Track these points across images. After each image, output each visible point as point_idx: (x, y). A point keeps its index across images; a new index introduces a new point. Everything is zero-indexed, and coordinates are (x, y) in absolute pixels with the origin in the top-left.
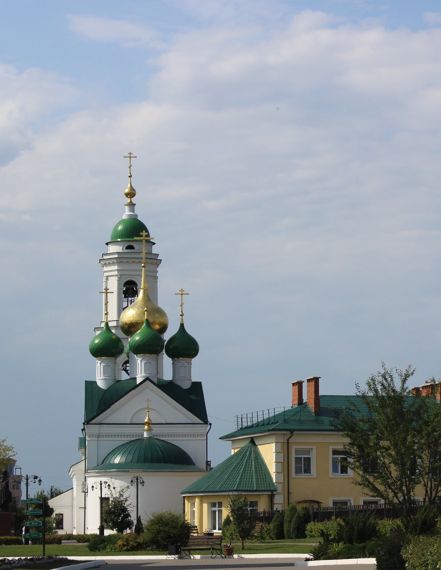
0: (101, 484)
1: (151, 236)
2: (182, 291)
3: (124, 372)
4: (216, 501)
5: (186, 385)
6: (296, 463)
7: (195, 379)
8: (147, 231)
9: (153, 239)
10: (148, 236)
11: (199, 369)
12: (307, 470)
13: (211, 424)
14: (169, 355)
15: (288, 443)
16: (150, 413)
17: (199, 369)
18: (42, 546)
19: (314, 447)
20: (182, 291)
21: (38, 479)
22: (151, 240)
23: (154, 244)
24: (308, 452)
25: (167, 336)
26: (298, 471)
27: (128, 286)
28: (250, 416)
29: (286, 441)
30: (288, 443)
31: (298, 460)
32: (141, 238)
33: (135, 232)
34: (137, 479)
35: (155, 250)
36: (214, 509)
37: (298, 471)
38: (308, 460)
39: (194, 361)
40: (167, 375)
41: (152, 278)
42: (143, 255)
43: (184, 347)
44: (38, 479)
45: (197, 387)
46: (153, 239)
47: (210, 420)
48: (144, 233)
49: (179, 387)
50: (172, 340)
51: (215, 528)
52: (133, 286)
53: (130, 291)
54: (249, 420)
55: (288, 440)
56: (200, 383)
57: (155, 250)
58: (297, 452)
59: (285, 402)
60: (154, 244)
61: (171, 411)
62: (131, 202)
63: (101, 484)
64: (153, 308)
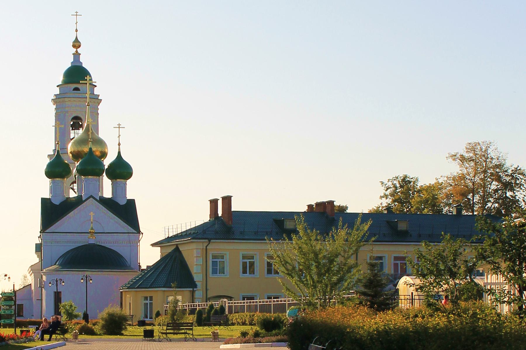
0: (57, 281)
1: (93, 81)
2: (119, 125)
3: (71, 190)
4: (148, 295)
5: (122, 202)
6: (213, 266)
7: (129, 197)
8: (90, 76)
9: (95, 82)
10: (91, 80)
11: (133, 189)
12: (252, 272)
13: (142, 234)
14: (110, 176)
15: (206, 249)
16: (89, 224)
17: (133, 189)
18: (14, 329)
19: (228, 253)
20: (119, 125)
21: (8, 277)
22: (94, 84)
23: (96, 86)
24: (252, 257)
25: (107, 162)
26: (214, 272)
27: (75, 121)
28: (175, 227)
29: (205, 248)
30: (206, 249)
31: (214, 264)
32: (86, 82)
33: (76, 75)
34: (86, 278)
35: (96, 91)
36: (147, 302)
37: (214, 272)
38: (252, 264)
39: (129, 182)
40: (107, 193)
41: (95, 115)
42: (88, 96)
43: (121, 171)
44: (8, 277)
45: (132, 203)
46: (95, 82)
47: (142, 230)
48: (88, 78)
49: (117, 204)
50: (111, 165)
51: (147, 317)
52: (78, 121)
53: (77, 125)
54: (174, 230)
55: (206, 247)
56: (134, 200)
57: (96, 91)
58: (214, 257)
59: (203, 217)
60: (96, 86)
61: (113, 222)
62: (77, 51)
63: (57, 281)
64: (92, 137)
